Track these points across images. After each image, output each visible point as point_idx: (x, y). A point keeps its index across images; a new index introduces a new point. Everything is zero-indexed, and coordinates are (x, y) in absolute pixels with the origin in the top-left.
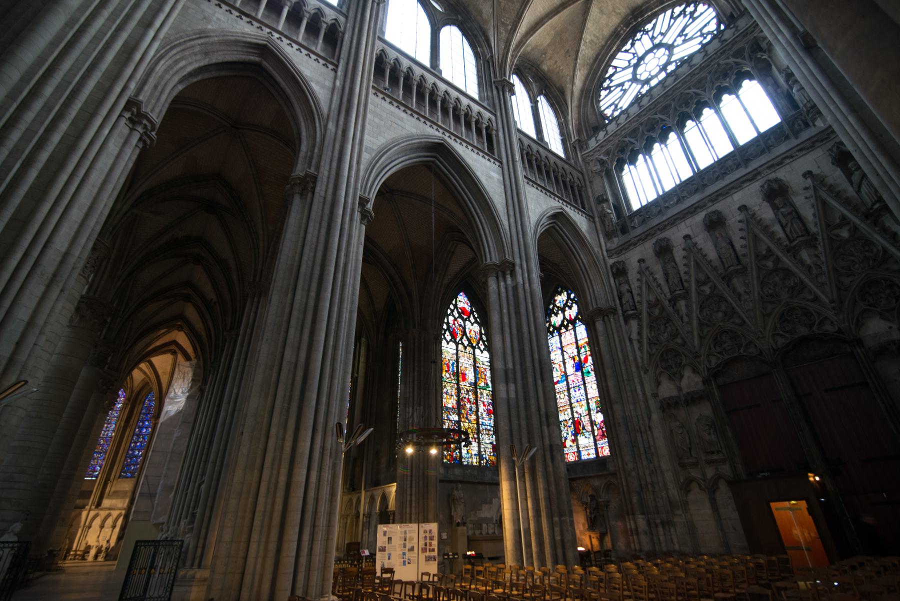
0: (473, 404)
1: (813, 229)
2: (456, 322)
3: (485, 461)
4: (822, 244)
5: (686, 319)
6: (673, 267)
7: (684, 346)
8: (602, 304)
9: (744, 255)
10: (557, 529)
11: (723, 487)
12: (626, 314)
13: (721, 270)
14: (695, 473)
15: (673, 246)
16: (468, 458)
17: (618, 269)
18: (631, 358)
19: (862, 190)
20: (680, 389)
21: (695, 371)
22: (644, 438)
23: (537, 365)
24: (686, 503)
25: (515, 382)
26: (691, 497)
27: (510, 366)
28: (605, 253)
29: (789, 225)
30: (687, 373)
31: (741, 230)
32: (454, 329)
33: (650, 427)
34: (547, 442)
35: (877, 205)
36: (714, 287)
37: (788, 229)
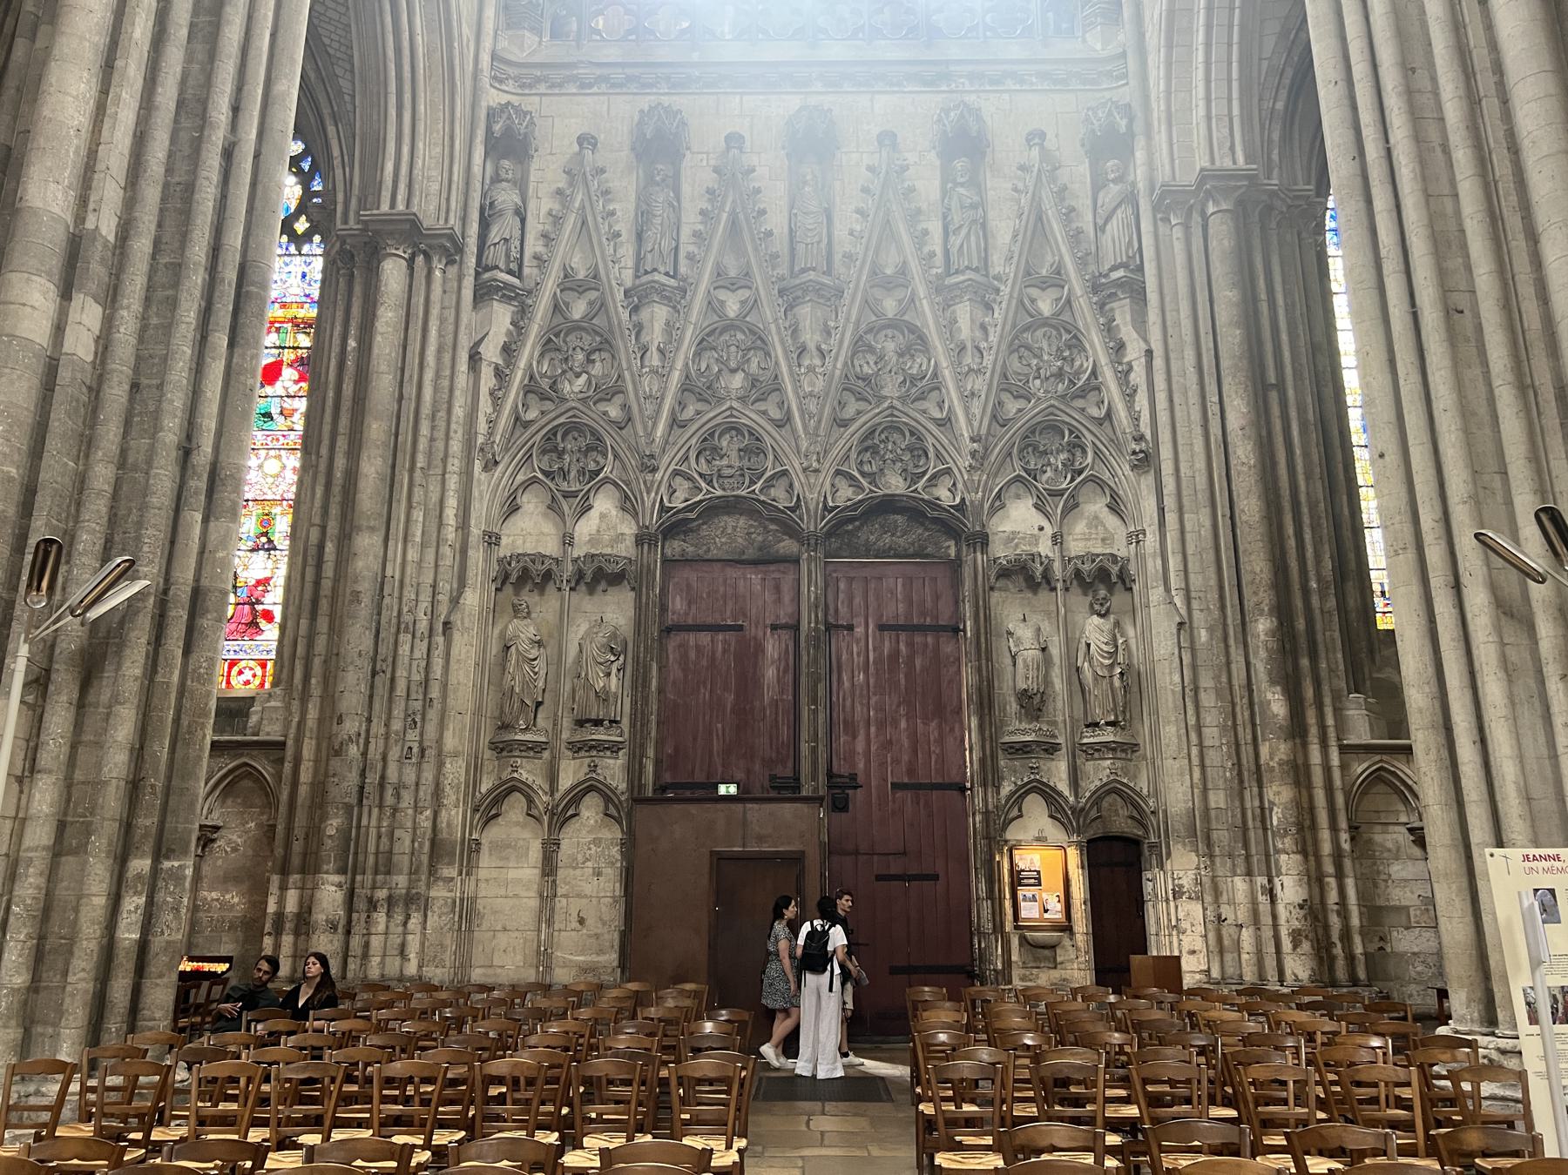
1: (998, 265)
4: (1004, 305)
5: (654, 359)
6: (671, 205)
7: (621, 429)
8: (428, 212)
9: (849, 257)
10: (133, 903)
11: (591, 810)
12: (487, 276)
13: (783, 270)
14: (529, 772)
15: (688, 148)
17: (508, 131)
18: (459, 412)
19: (1109, 227)
20: (567, 540)
21: (628, 504)
22: (417, 654)
23: (230, 275)
24: (474, 848)
25: (111, 298)
26: (495, 832)
27: (106, 224)
28: (485, 59)
29: (964, 232)
30: (604, 503)
31: (865, 190)
33: (447, 624)
34: (185, 574)
35: (1120, 273)
36: (753, 305)
37: (956, 241)
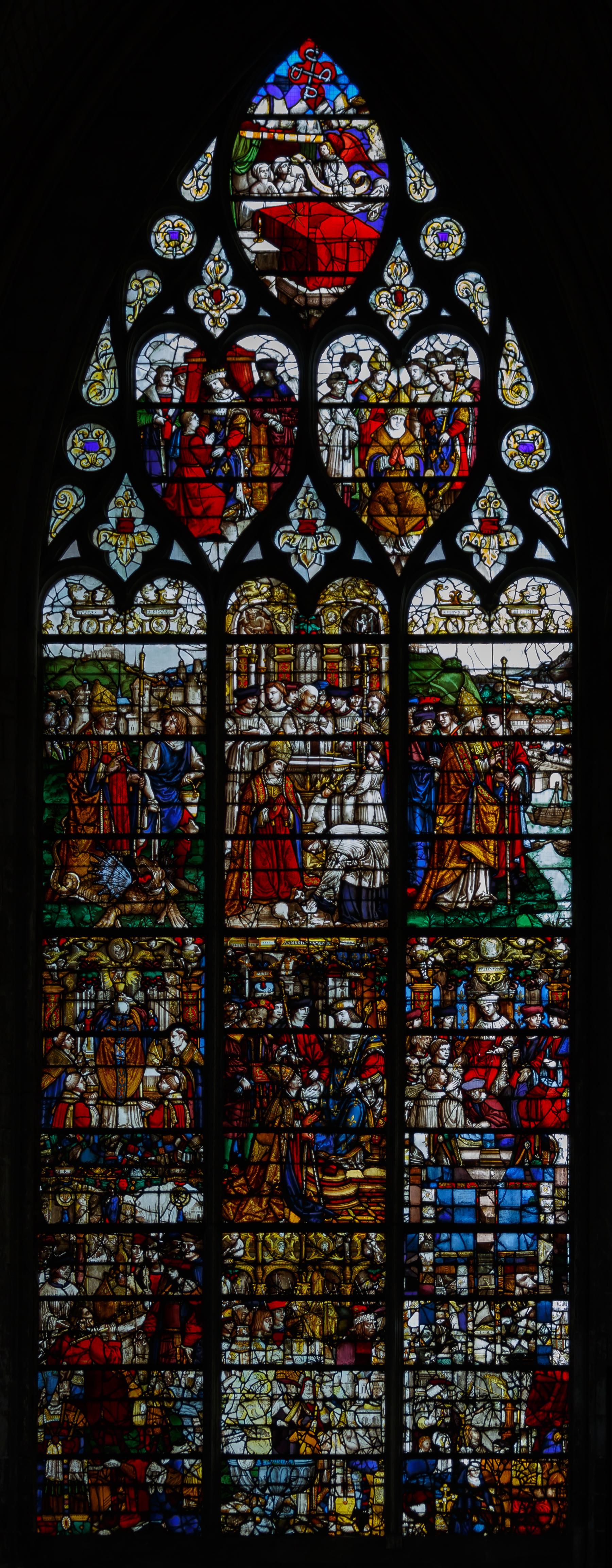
0: (359, 1070)
2: (216, 380)
3: (446, 1501)
16: (289, 1488)
32: (193, 444)
